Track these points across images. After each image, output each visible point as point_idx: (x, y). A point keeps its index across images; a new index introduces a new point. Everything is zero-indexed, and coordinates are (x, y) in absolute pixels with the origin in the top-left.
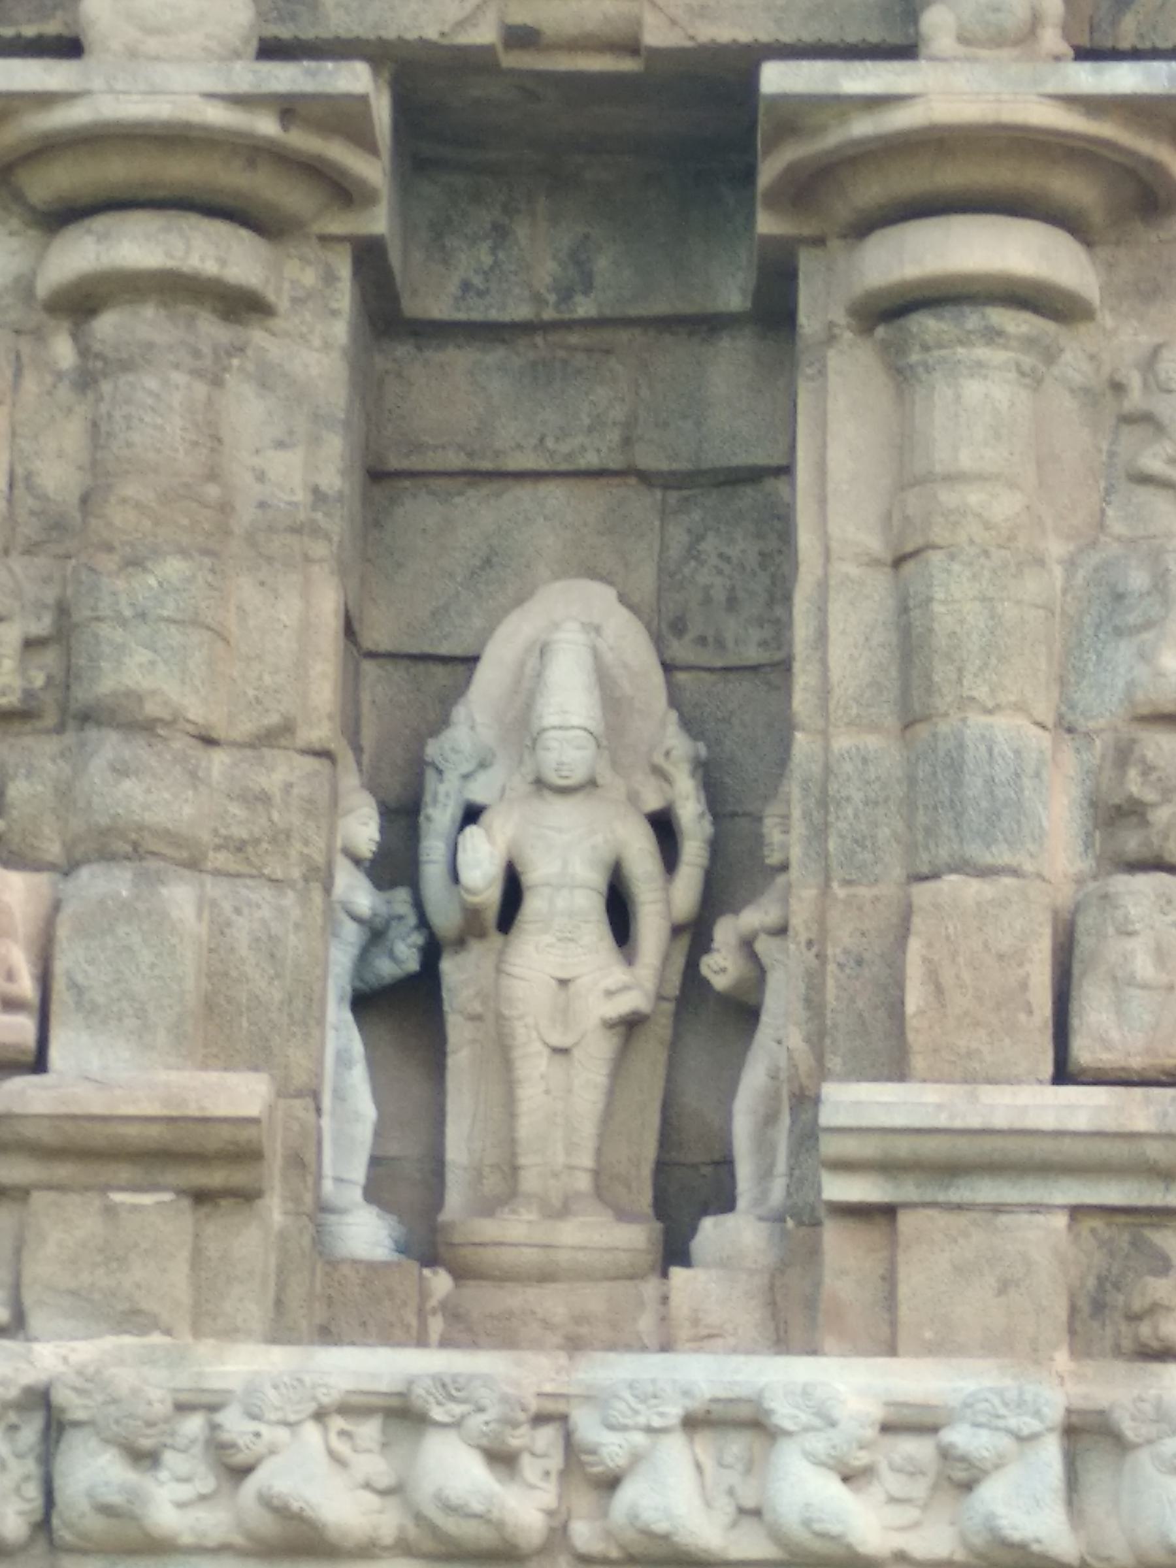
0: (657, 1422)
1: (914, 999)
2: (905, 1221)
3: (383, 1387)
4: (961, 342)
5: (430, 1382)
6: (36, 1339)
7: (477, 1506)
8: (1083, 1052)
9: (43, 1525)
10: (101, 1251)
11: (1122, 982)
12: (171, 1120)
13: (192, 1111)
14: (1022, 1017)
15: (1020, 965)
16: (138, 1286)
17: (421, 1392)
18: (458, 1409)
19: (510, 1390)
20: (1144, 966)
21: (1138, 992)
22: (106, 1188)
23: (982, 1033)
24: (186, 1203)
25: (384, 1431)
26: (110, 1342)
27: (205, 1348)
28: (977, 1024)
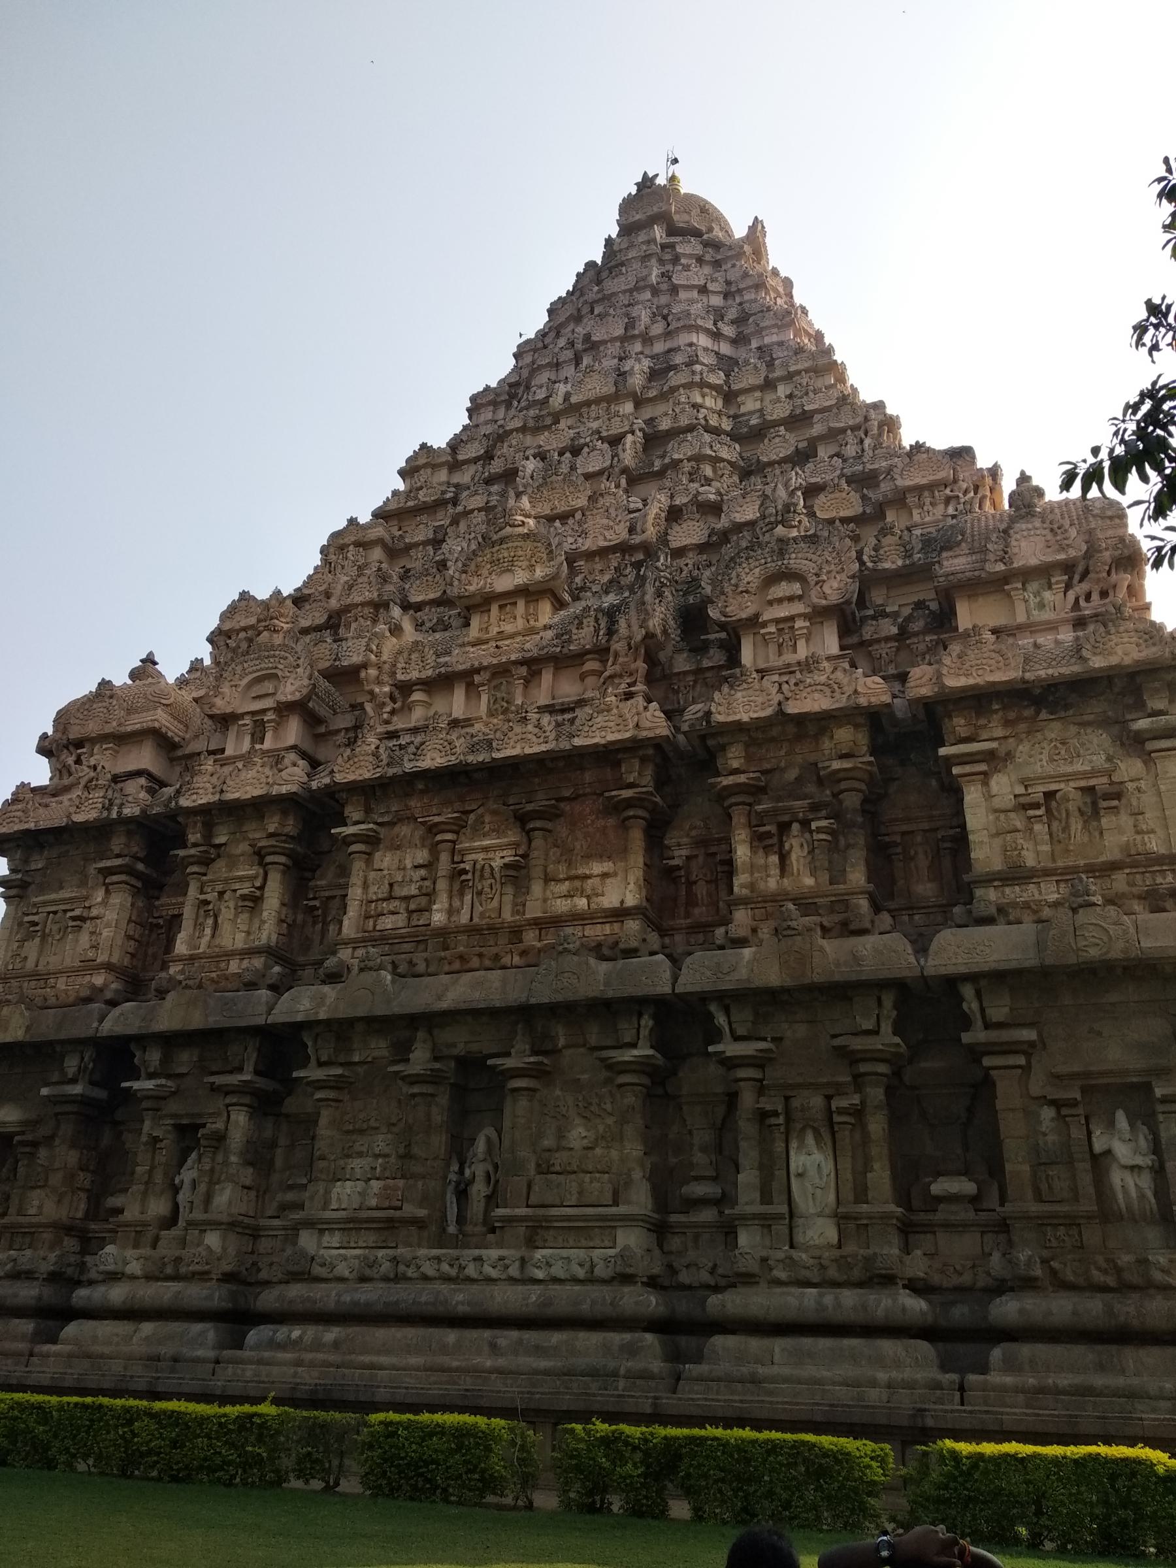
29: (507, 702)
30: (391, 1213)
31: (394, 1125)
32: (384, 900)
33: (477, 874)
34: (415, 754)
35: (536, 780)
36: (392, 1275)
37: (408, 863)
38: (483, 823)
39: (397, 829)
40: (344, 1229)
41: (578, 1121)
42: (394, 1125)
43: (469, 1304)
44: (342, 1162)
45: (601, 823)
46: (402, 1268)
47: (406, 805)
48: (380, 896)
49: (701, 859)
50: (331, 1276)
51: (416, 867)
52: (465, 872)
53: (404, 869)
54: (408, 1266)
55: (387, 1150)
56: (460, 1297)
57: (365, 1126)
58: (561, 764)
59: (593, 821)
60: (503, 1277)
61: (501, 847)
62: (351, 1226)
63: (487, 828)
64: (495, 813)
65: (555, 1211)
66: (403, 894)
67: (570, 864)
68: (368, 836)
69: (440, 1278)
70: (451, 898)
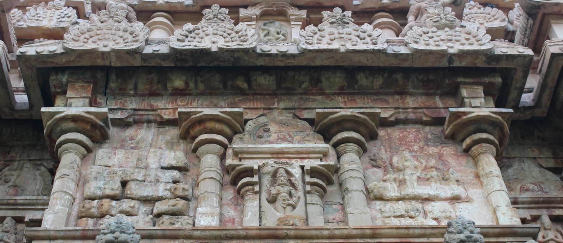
29: (283, 35)
32: (113, 198)
33: (266, 180)
34: (187, 37)
35: (340, 99)
37: (153, 162)
38: (268, 131)
39: (130, 132)
45: (433, 150)
47: (152, 106)
48: (108, 192)
49: (546, 220)
51: (163, 168)
52: (250, 172)
53: (146, 168)
58: (378, 82)
59: (422, 148)
61: (302, 155)
63: (274, 136)
64: (282, 124)
66: (145, 194)
67: (402, 183)
68: (94, 125)
70: (221, 206)
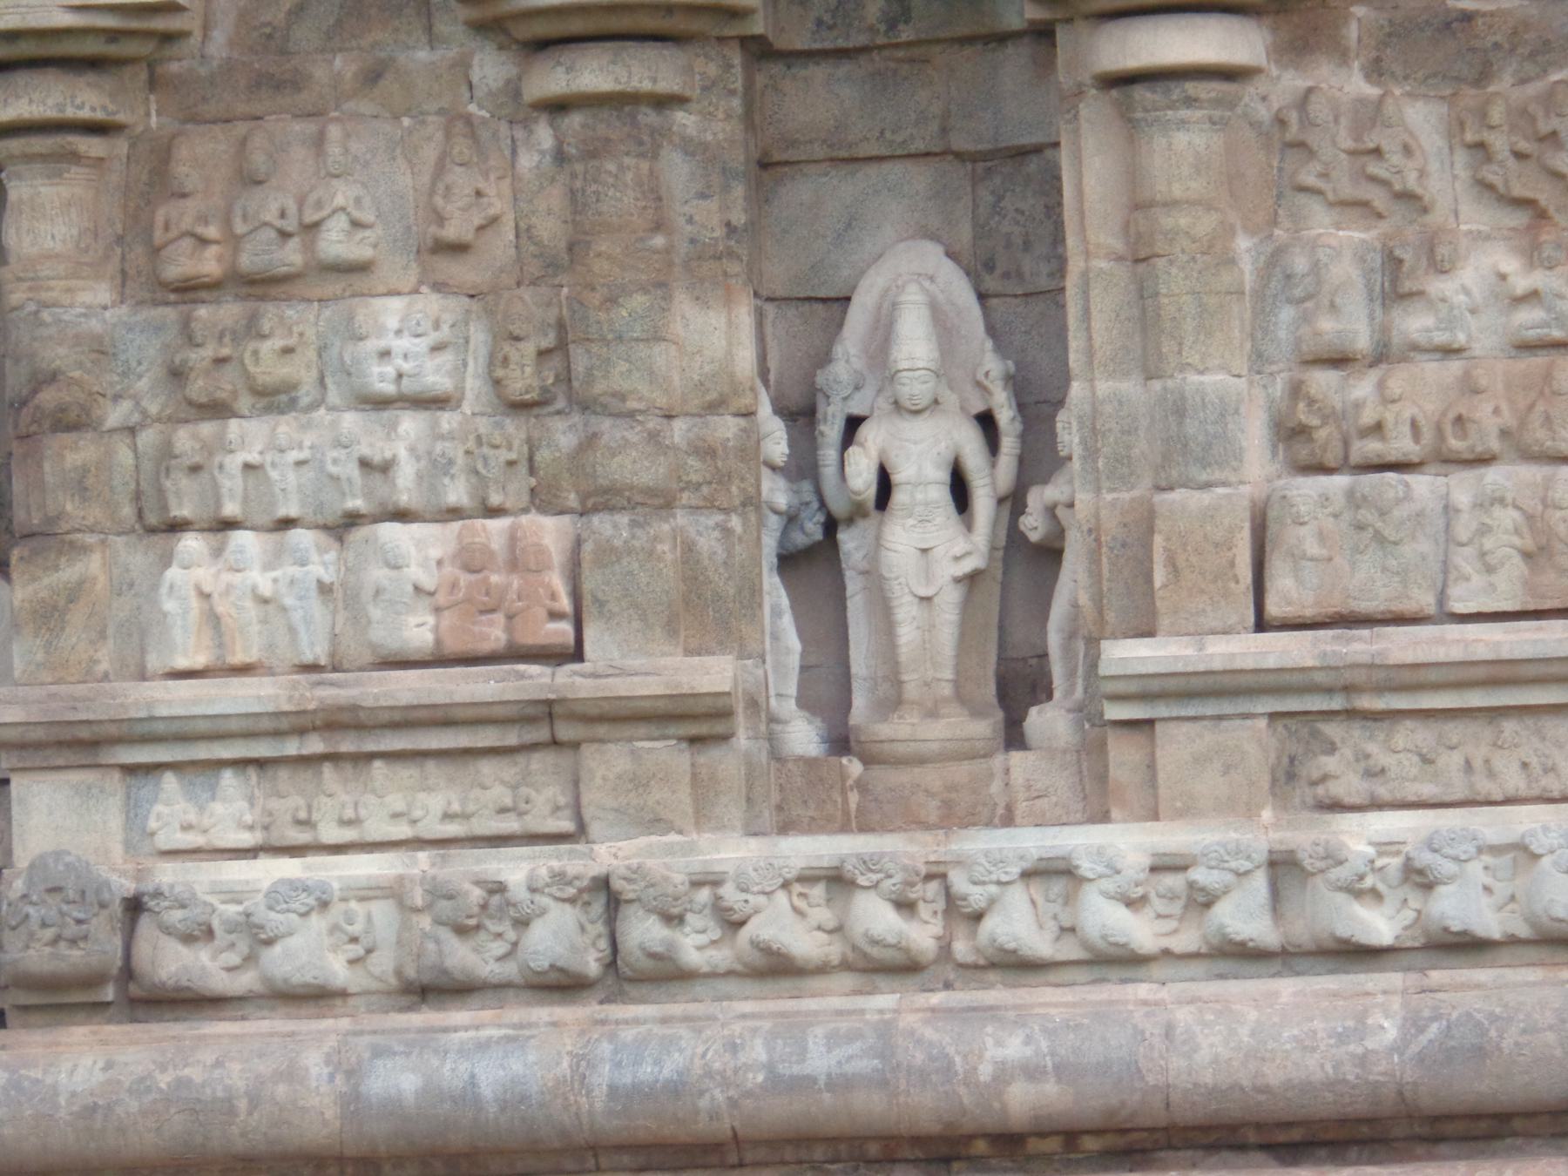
0: (1004, 878)
1: (1159, 577)
2: (1158, 727)
3: (825, 865)
4: (1170, 108)
5: (855, 860)
6: (594, 842)
7: (891, 940)
8: (1273, 609)
9: (612, 963)
10: (631, 781)
11: (1297, 558)
12: (671, 696)
13: (685, 690)
14: (1232, 585)
15: (1230, 549)
16: (658, 803)
17: (850, 867)
18: (875, 877)
19: (906, 861)
20: (1312, 548)
21: (1309, 563)
22: (630, 740)
23: (1205, 597)
24: (684, 745)
25: (828, 891)
26: (643, 841)
27: (705, 839)
28: (1202, 591)
30: (537, 680)
31: (458, 249)
36: (592, 965)
40: (260, 763)
41: (1475, 217)
42: (458, 249)
43: (1060, 1070)
44: (185, 440)
46: (643, 932)
50: (245, 981)
54: (673, 919)
55: (435, 376)
56: (1014, 1048)
57: (292, 256)
60: (1188, 940)
62: (315, 745)
65: (1400, 645)
69: (846, 966)
